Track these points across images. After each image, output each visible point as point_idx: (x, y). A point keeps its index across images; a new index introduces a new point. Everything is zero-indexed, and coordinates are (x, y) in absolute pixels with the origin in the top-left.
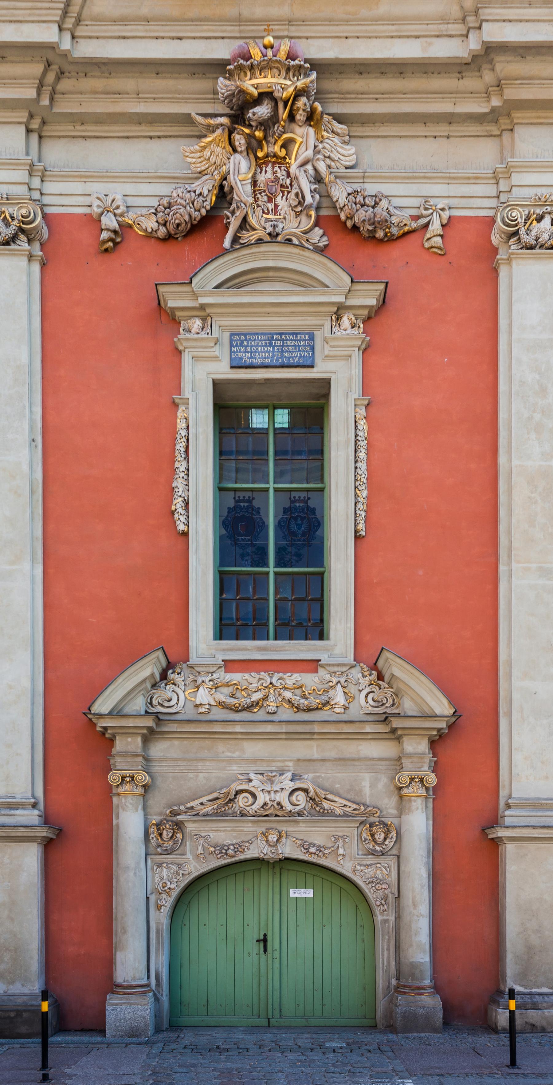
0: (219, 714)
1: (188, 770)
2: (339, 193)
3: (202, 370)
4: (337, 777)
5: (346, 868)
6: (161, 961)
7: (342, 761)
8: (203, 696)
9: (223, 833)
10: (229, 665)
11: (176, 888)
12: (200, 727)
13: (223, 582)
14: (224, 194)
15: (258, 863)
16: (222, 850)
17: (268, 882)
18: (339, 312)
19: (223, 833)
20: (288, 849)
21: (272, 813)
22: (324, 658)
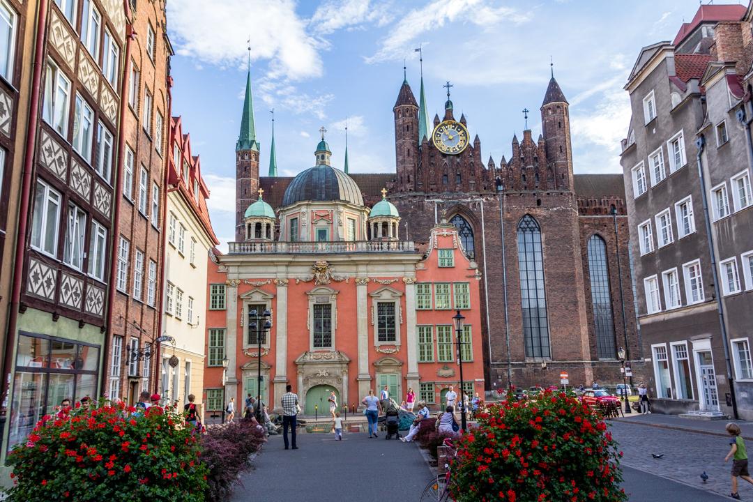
0: (314, 360)
1: (309, 370)
2: (333, 277)
3: (311, 305)
4: (332, 371)
5: (334, 386)
6: (304, 402)
7: (334, 368)
8: (312, 357)
9: (315, 381)
10: (316, 352)
11: (307, 390)
12: (312, 363)
13: (315, 336)
14: (315, 277)
15: (320, 386)
16: (314, 383)
17: (322, 389)
18: (332, 294)
19: (315, 381)
20: (325, 383)
21: (323, 377)
22: (331, 350)
